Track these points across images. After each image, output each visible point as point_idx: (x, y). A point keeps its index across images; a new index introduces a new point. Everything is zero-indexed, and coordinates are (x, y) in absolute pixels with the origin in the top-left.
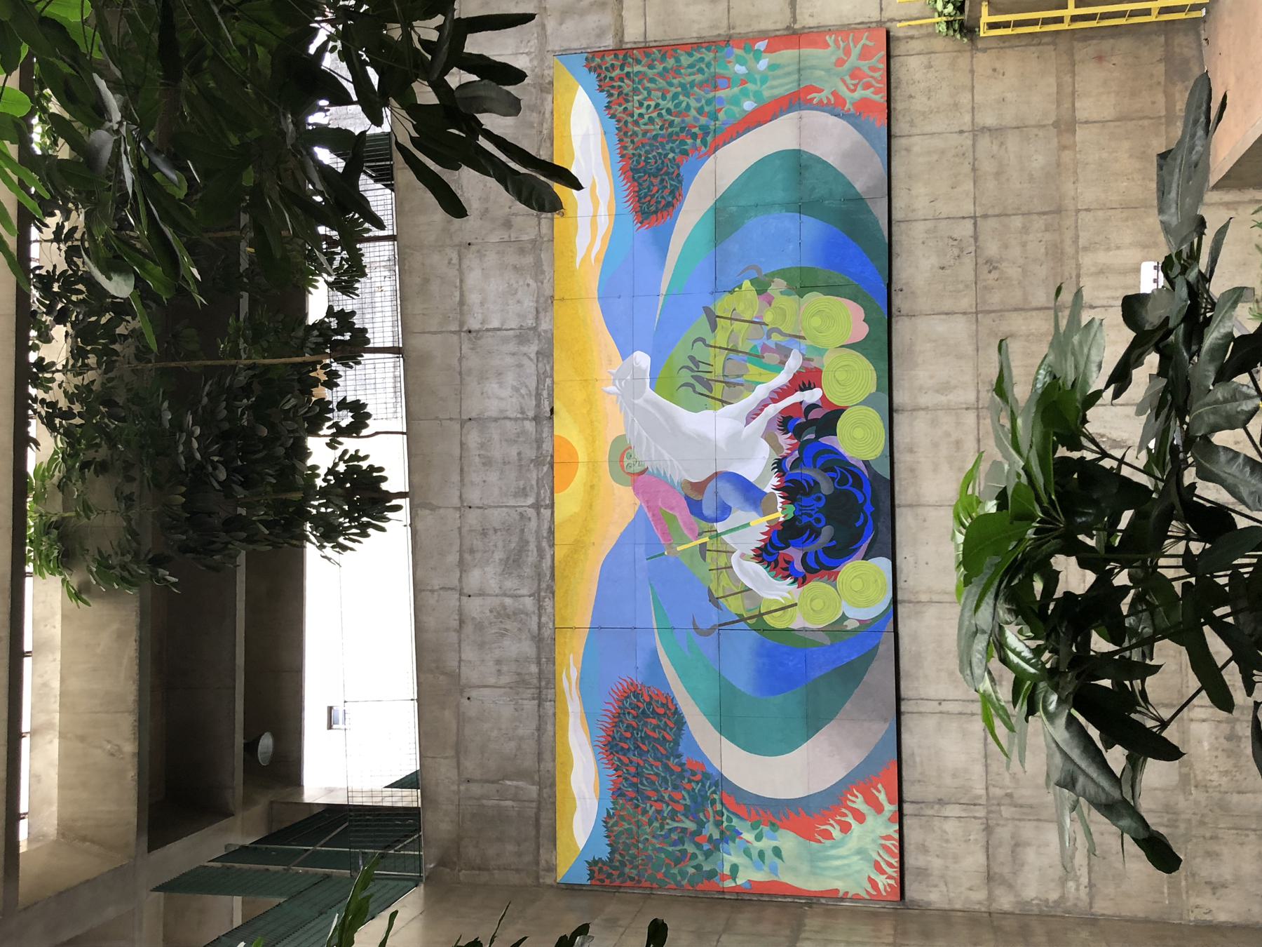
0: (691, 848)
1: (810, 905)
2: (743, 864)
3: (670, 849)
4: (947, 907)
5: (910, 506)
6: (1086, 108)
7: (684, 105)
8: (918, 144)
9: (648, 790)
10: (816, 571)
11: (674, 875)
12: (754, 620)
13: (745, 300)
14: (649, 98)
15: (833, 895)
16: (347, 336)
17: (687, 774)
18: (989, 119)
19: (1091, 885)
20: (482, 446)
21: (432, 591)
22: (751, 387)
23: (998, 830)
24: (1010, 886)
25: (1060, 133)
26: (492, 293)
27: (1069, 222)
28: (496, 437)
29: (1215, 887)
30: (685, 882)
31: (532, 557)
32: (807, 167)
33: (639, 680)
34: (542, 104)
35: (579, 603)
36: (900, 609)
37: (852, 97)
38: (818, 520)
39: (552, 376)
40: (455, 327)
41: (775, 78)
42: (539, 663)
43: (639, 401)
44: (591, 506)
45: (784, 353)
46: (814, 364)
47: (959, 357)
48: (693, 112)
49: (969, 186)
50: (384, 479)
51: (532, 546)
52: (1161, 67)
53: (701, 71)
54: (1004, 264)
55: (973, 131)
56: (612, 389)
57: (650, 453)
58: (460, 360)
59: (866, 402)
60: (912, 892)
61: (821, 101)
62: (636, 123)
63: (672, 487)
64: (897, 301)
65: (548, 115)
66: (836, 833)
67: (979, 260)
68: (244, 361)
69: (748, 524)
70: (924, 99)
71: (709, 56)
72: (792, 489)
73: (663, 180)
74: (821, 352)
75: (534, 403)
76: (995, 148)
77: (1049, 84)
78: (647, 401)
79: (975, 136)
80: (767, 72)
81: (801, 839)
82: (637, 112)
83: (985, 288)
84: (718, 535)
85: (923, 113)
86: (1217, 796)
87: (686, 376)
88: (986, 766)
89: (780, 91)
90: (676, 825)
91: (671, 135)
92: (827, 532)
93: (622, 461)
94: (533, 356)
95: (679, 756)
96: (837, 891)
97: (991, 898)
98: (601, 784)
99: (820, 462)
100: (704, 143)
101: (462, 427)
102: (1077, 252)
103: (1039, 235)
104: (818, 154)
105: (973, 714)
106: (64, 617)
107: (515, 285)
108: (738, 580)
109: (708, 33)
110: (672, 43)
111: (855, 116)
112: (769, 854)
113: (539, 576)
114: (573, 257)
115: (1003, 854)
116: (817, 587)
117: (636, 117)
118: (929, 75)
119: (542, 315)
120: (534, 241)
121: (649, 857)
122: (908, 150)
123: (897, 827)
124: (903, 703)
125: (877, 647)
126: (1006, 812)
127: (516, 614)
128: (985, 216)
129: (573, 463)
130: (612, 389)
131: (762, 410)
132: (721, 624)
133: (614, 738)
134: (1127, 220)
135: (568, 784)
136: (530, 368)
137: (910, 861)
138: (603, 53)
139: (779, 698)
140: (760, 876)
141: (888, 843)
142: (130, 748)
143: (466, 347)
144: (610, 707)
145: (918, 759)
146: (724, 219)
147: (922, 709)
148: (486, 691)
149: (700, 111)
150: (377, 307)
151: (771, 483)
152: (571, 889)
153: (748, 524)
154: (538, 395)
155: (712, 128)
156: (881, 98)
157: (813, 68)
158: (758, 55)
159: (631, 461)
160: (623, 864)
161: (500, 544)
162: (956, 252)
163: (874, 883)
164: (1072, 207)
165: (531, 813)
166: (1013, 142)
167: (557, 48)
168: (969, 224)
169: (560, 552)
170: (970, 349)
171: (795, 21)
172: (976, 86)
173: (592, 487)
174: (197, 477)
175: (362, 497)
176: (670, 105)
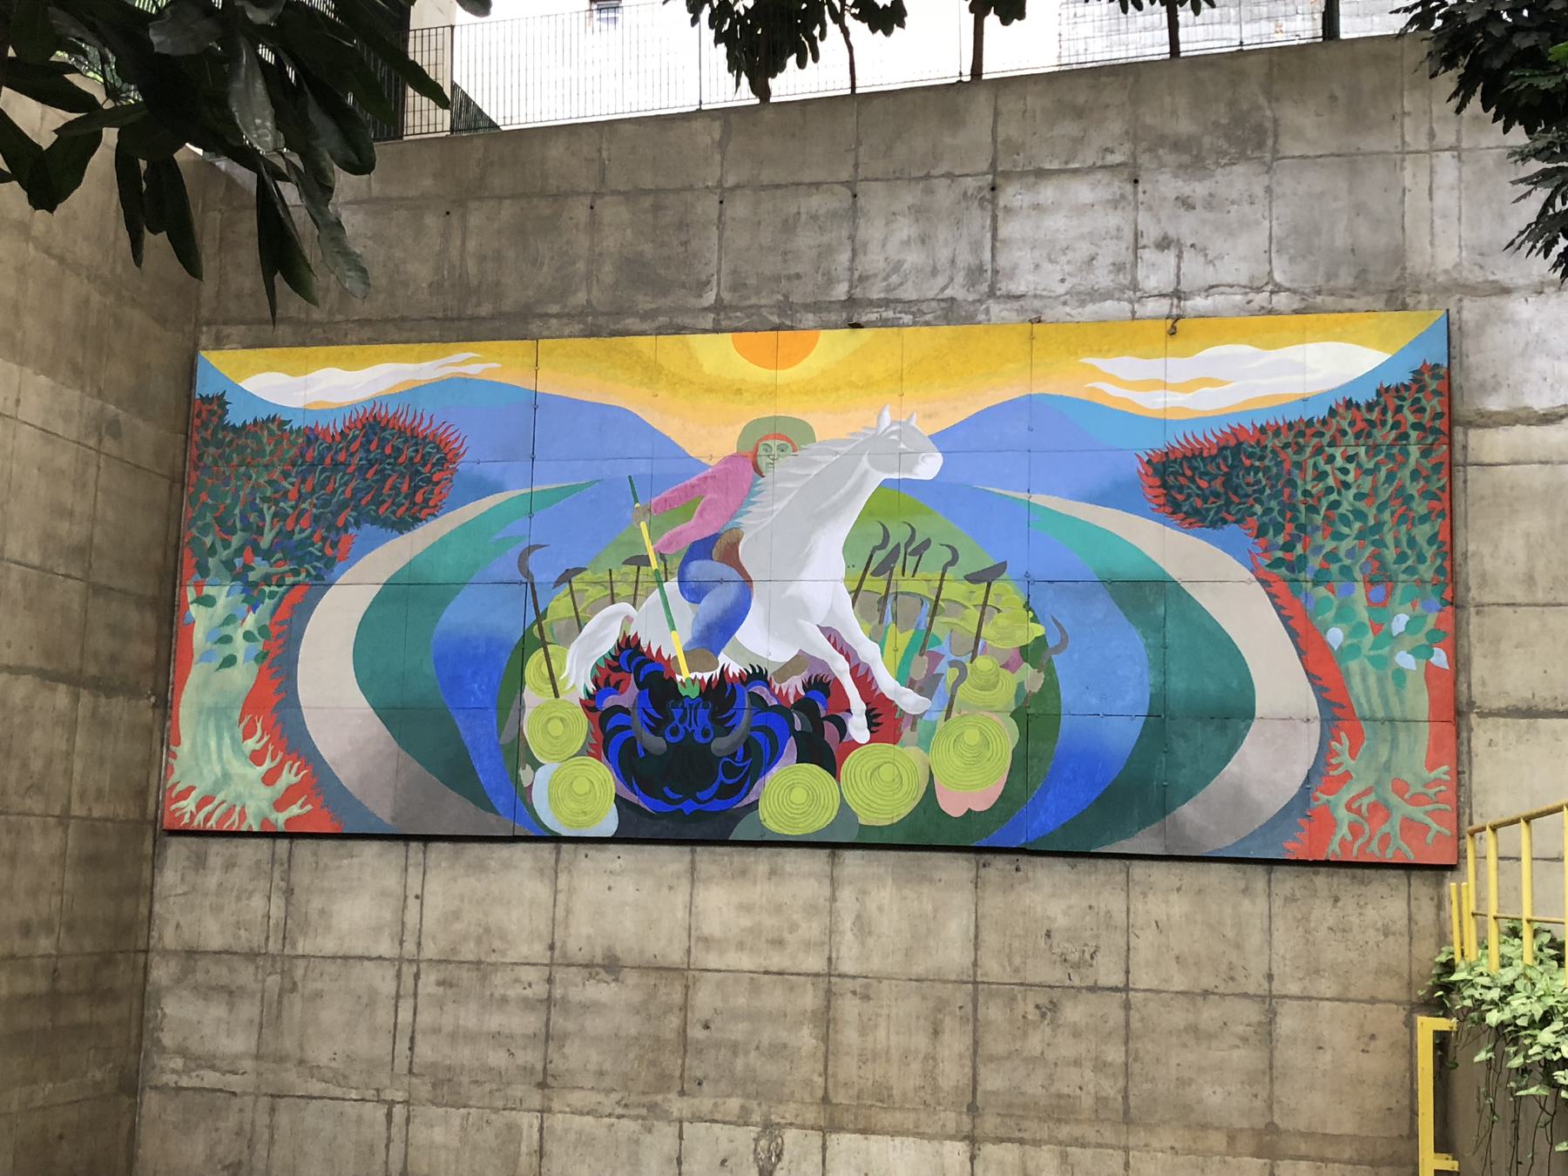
0: (236, 541)
2: (215, 614)
3: (237, 511)
4: (156, 891)
5: (693, 868)
7: (1345, 530)
8: (1253, 908)
9: (315, 478)
10: (602, 727)
12: (537, 634)
14: (1362, 471)
17: (333, 536)
18: (1287, 1023)
19: (179, 1089)
20: (814, 217)
21: (600, 150)
22: (877, 636)
23: (251, 969)
24: (178, 981)
25: (1257, 1133)
26: (1061, 226)
27: (1108, 1135)
30: (194, 531)
31: (644, 302)
32: (1223, 729)
34: (1368, 293)
35: (569, 371)
36: (546, 849)
37: (1339, 805)
38: (674, 732)
39: (915, 324)
41: (1380, 680)
42: (492, 318)
43: (865, 463)
44: (710, 390)
45: (926, 687)
46: (907, 733)
47: (908, 953)
48: (1330, 545)
49: (1179, 983)
50: (801, 64)
53: (1402, 557)
54: (1048, 1030)
55: (1271, 997)
56: (887, 417)
57: (785, 481)
58: (950, 175)
59: (844, 806)
60: (177, 850)
61: (1336, 754)
62: (1318, 450)
63: (733, 516)
64: (1000, 863)
65: (1348, 303)
66: (251, 744)
67: (1056, 993)
69: (673, 628)
70: (1331, 922)
71: (1426, 572)
72: (721, 693)
73: (1217, 495)
74: (925, 744)
75: (875, 297)
76: (1240, 1029)
79: (1262, 998)
81: (243, 697)
82: (1338, 452)
83: (1014, 999)
84: (660, 583)
87: (899, 535)
88: (334, 958)
90: (268, 519)
91: (1294, 509)
92: (657, 744)
93: (777, 436)
94: (948, 293)
95: (357, 524)
96: (178, 744)
97: (166, 953)
98: (322, 412)
99: (758, 736)
100: (1276, 563)
101: (845, 183)
102: (1060, 1143)
104: (1246, 747)
105: (401, 943)
107: (1063, 259)
108: (594, 613)
109: (1471, 572)
112: (227, 650)
114: (1100, 352)
116: (580, 727)
117: (1330, 450)
118: (1371, 932)
120: (1135, 286)
121: (226, 482)
122: (1245, 891)
123: (255, 829)
124: (421, 845)
125: (492, 810)
126: (273, 981)
128: (1127, 1006)
130: (887, 417)
131: (841, 652)
133: (384, 429)
135: (327, 362)
136: (932, 289)
137: (216, 847)
138: (1448, 392)
139: (429, 669)
140: (199, 636)
141: (235, 816)
143: (970, 183)
144: (426, 423)
145: (345, 862)
146: (1146, 596)
147: (410, 869)
149: (1332, 556)
151: (731, 663)
152: (189, 371)
153: (673, 628)
154: (886, 303)
155: (1302, 576)
156: (1333, 851)
157: (1394, 745)
158: (1419, 652)
159: (775, 451)
160: (220, 444)
162: (1075, 957)
163: (185, 794)
166: (1246, 1058)
167: (1466, 315)
168: (1117, 979)
170: (918, 969)
171: (1482, 715)
172: (1344, 1008)
173: (739, 391)
176: (1345, 508)
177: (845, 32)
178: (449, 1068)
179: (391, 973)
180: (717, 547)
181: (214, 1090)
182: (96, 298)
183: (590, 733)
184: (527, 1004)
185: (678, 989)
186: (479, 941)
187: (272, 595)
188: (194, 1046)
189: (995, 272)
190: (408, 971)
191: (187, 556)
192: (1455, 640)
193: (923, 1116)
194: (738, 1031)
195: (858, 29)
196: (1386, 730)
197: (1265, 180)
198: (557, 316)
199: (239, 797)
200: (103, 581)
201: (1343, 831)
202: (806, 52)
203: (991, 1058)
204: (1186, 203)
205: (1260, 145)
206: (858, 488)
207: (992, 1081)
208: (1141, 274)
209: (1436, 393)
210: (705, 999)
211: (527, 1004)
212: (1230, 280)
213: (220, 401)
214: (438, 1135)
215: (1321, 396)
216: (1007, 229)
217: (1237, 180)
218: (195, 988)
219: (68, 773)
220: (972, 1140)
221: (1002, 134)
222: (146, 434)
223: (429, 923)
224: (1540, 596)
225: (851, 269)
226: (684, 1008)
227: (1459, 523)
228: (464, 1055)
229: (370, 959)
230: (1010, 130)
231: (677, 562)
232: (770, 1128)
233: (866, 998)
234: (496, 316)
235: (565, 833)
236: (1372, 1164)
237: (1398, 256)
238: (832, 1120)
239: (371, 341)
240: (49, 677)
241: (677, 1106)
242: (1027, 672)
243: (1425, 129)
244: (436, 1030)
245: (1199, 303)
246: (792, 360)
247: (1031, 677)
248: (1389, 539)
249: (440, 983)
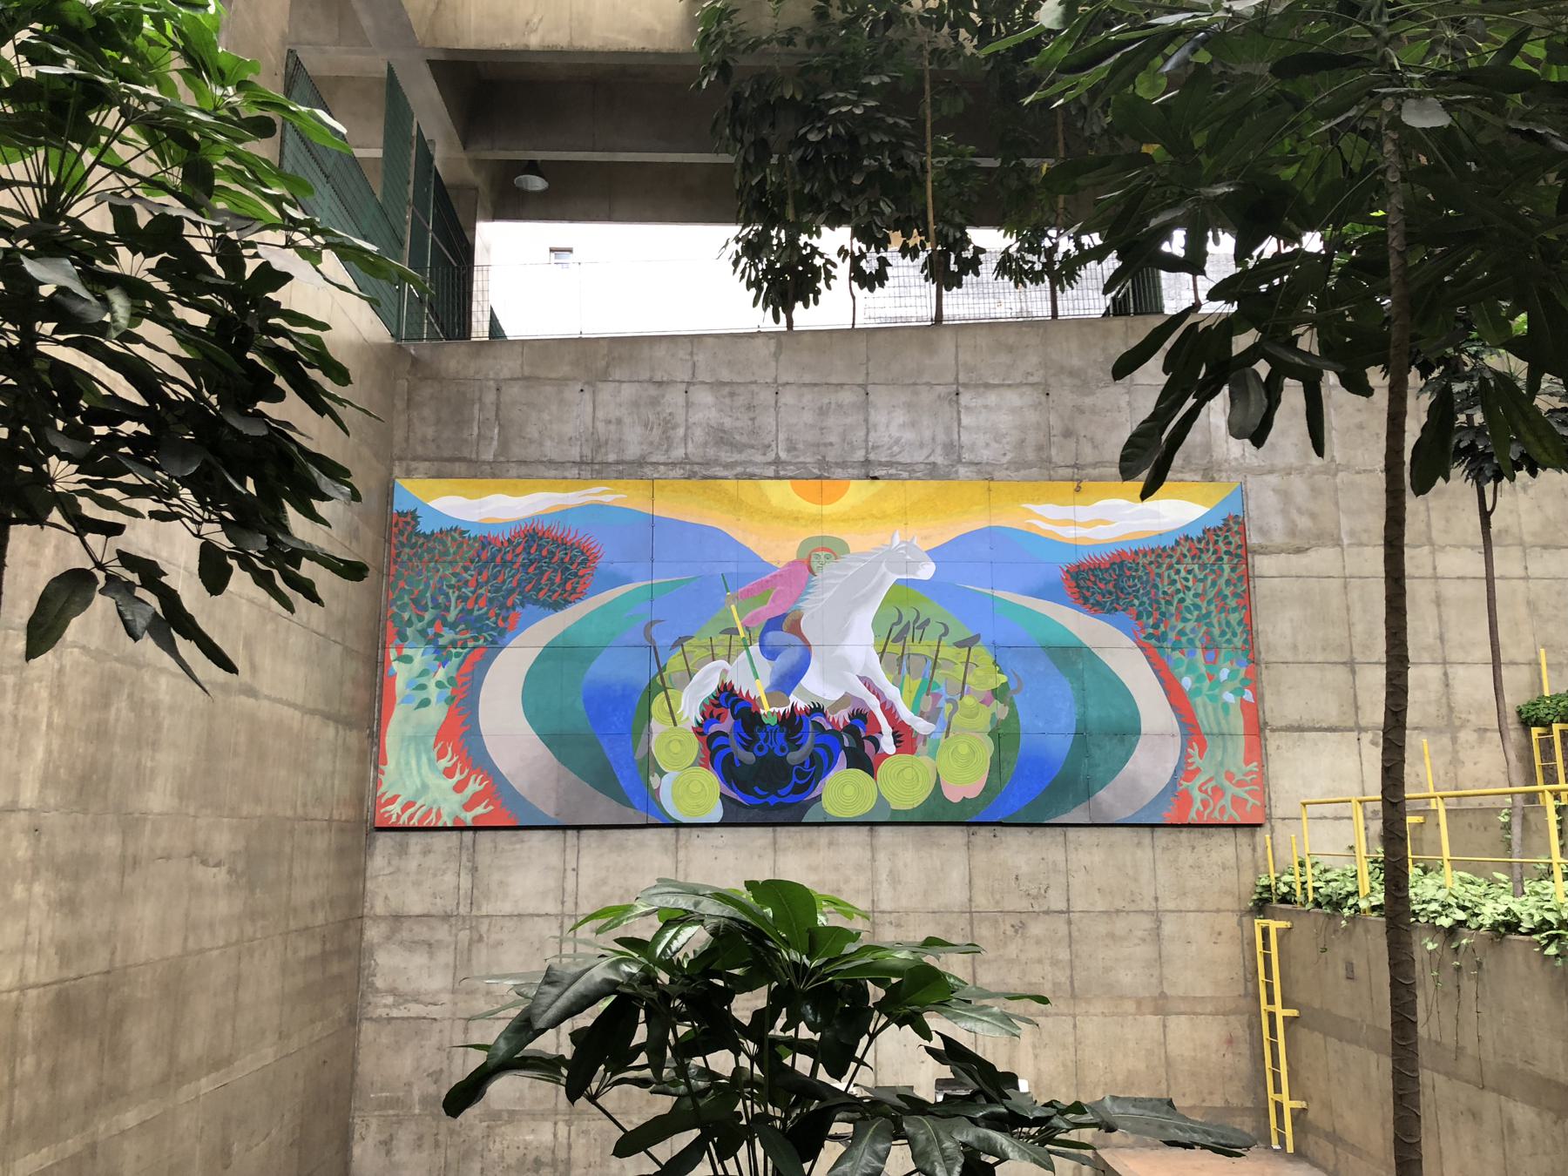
0: (428, 616)
1: (371, 735)
2: (412, 669)
6: (1179, 1025)
8: (1144, 855)
9: (488, 572)
11: (401, 598)
13: (986, 677)
14: (1196, 580)
15: (379, 760)
16: (954, 268)
17: (504, 612)
18: (1168, 928)
19: (390, 1019)
20: (840, 406)
21: (692, 354)
22: (898, 683)
23: (446, 927)
24: (388, 938)
25: (1155, 999)
26: (996, 418)
28: (849, 420)
29: (387, 1144)
30: (394, 609)
31: (726, 456)
32: (1122, 741)
33: (600, 564)
35: (678, 504)
36: (670, 831)
37: (1193, 787)
38: (761, 749)
40: (962, 379)
41: (1215, 709)
42: (618, 463)
43: (884, 568)
45: (931, 717)
47: (926, 893)
48: (1180, 625)
50: (806, 306)
51: (736, 457)
52: (1219, 1103)
53: (1223, 633)
56: (897, 541)
57: (830, 581)
58: (928, 384)
59: (880, 797)
60: (383, 840)
62: (1170, 567)
63: (796, 601)
64: (984, 832)
65: (1180, 476)
66: (445, 763)
68: (929, 161)
70: (1191, 862)
71: (1238, 642)
72: (792, 723)
73: (1110, 593)
76: (1140, 933)
77: (1205, 989)
78: (884, 575)
79: (1152, 913)
80: (1221, 703)
82: (1182, 568)
84: (746, 647)
85: (1176, 860)
87: (909, 616)
89: (1201, 715)
92: (748, 757)
93: (823, 549)
94: (932, 459)
95: (522, 605)
97: (376, 918)
99: (819, 750)
100: (1149, 636)
103: (1050, 977)
104: (1136, 752)
105: (563, 903)
109: (1261, 642)
111: (1174, 790)
112: (423, 695)
113: (707, 464)
114: (1033, 501)
115: (422, 932)
116: (694, 746)
119: (973, 468)
124: (575, 832)
125: (631, 806)
126: (464, 935)
127: (668, 440)
128: (1069, 922)
129: (822, 499)
130: (897, 541)
134: (1064, 1065)
136: (919, 456)
137: (414, 838)
138: (1243, 532)
139: (580, 706)
140: (400, 684)
141: (433, 816)
142: (534, 42)
146: (1070, 657)
147: (568, 851)
148: (589, 409)
149: (1182, 633)
150: (984, 299)
151: (798, 701)
152: (388, 492)
154: (890, 464)
156: (1192, 817)
157: (1225, 750)
160: (413, 547)
161: (738, 424)
165: (466, 454)
166: (1145, 951)
168: (1062, 906)
169: (730, 485)
170: (933, 906)
171: (1273, 730)
173: (796, 519)
175: (789, 283)
176: (1188, 602)
179: (555, 925)
181: (418, 1018)
183: (702, 751)
188: (402, 986)
191: (391, 628)
192: (1253, 680)
196: (1219, 741)
197: (1127, 397)
198: (664, 464)
199: (435, 801)
200: (348, 644)
201: (1197, 805)
206: (880, 584)
213: (413, 516)
215: (1168, 533)
216: (965, 420)
223: (583, 888)
224: (1301, 658)
229: (538, 916)
233: (898, 926)
239: (529, 477)
240: (327, 717)
246: (833, 499)
247: (1001, 710)
248: (1215, 621)
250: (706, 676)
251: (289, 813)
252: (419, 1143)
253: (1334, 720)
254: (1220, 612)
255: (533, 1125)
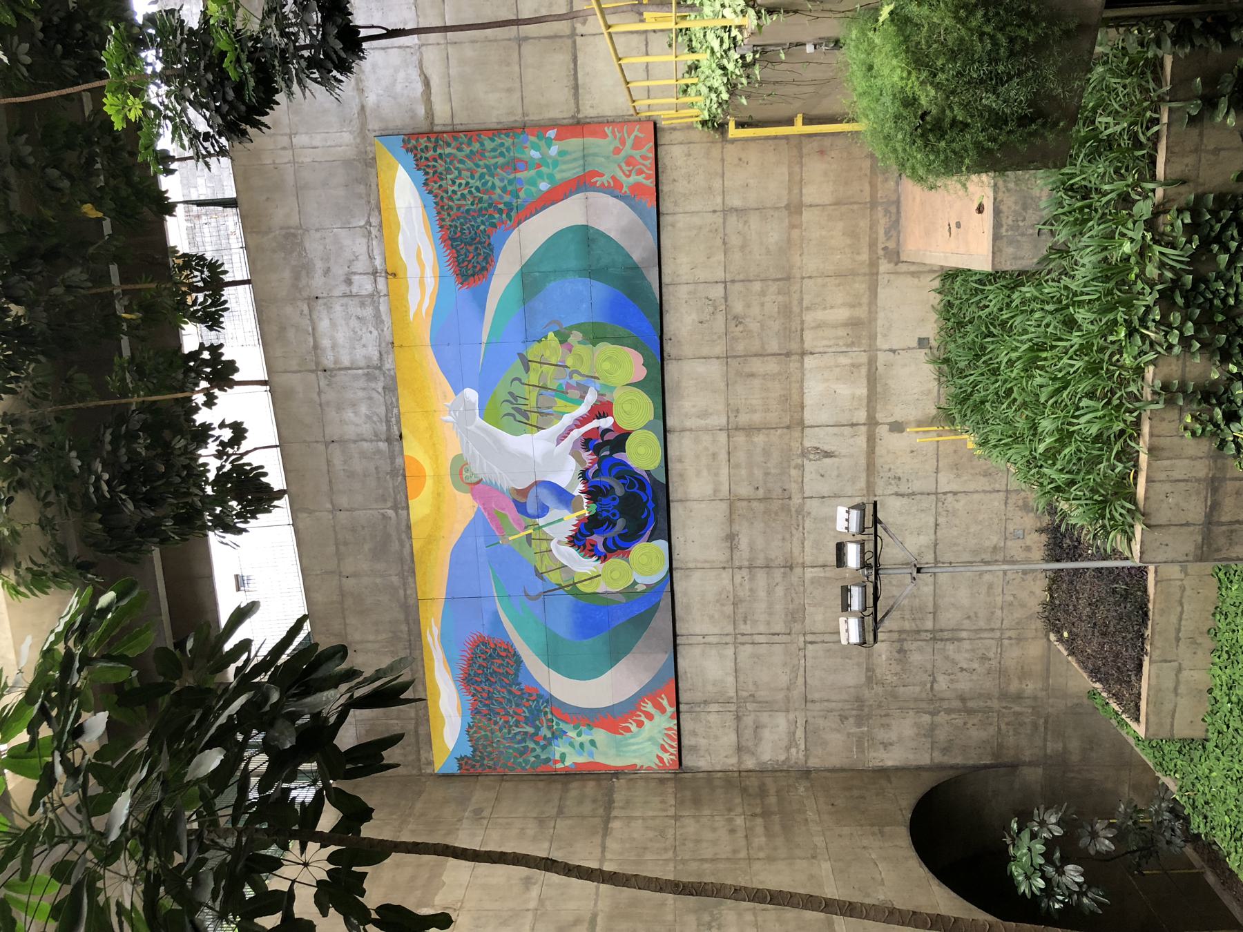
2: (569, 752)
5: (681, 501)
6: (811, 194)
7: (490, 184)
10: (614, 551)
13: (550, 347)
14: (460, 177)
18: (736, 202)
20: (345, 462)
22: (560, 416)
25: (790, 214)
26: (343, 335)
27: (796, 287)
29: (886, 745)
31: (395, 546)
33: (486, 633)
35: (434, 581)
36: (675, 574)
37: (628, 182)
38: (614, 515)
46: (607, 399)
48: (498, 191)
49: (722, 257)
50: (265, 474)
52: (868, 163)
53: (502, 154)
55: (724, 210)
57: (483, 467)
60: (688, 761)
61: (603, 184)
62: (450, 199)
64: (668, 348)
65: (374, 187)
66: (634, 727)
68: (134, 401)
70: (685, 182)
72: (594, 493)
73: (477, 248)
76: (740, 225)
78: (477, 427)
79: (725, 215)
82: (450, 189)
86: (889, 689)
87: (508, 408)
88: (736, 677)
92: (621, 523)
93: (461, 474)
94: (380, 390)
95: (519, 684)
97: (740, 762)
104: (602, 229)
106: (8, 605)
109: (508, 120)
110: (477, 127)
111: (630, 197)
112: (587, 745)
114: (407, 311)
115: (748, 733)
116: (615, 562)
120: (372, 295)
122: (673, 226)
126: (750, 706)
128: (733, 281)
129: (421, 476)
132: (545, 592)
134: (839, 285)
137: (685, 742)
138: (417, 135)
139: (590, 640)
140: (581, 760)
143: (323, 383)
146: (531, 280)
149: (504, 189)
150: (240, 338)
151: (578, 489)
154: (388, 422)
156: (650, 183)
157: (595, 155)
164: (798, 276)
166: (754, 220)
167: (376, 127)
168: (721, 286)
169: (416, 545)
170: (723, 385)
171: (578, 111)
173: (439, 494)
174: (110, 508)
175: (250, 493)
176: (478, 184)
177: (247, 453)
178: (786, 615)
179: (741, 647)
180: (520, 501)
182: (410, 827)
184: (752, 579)
185: (739, 504)
186: (723, 605)
187: (558, 724)
188: (784, 743)
189: (368, 367)
190: (741, 639)
191: (540, 770)
192: (540, 128)
193: (793, 379)
194: (758, 473)
195: (245, 446)
196: (590, 159)
197: (312, 232)
201: (641, 178)
202: (259, 472)
203: (763, 347)
204: (327, 271)
205: (295, 235)
207: (774, 346)
208: (364, 292)
209: (417, 140)
210: (744, 490)
211: (752, 579)
212: (365, 248)
213: (460, 760)
214: (819, 617)
216: (346, 363)
217: (314, 247)
218: (756, 745)
219: (653, 818)
220: (803, 354)
221: (296, 368)
222: (479, 796)
223: (716, 631)
224: (518, 85)
225: (372, 441)
226: (749, 500)
227: (483, 127)
228: (779, 607)
230: (294, 364)
231: (528, 519)
232: (804, 454)
233: (737, 411)
234: (407, 622)
235: (667, 566)
236: (801, 157)
237: (348, 163)
238: (798, 424)
240: (606, 831)
241: (796, 500)
242: (571, 340)
243: (282, 152)
244: (768, 623)
245: (378, 262)
246: (422, 469)
248: (493, 161)
249: (745, 623)
250: (563, 556)
251: (671, 865)
252: (886, 726)
253: (568, 57)
254: (482, 157)
255: (875, 655)
